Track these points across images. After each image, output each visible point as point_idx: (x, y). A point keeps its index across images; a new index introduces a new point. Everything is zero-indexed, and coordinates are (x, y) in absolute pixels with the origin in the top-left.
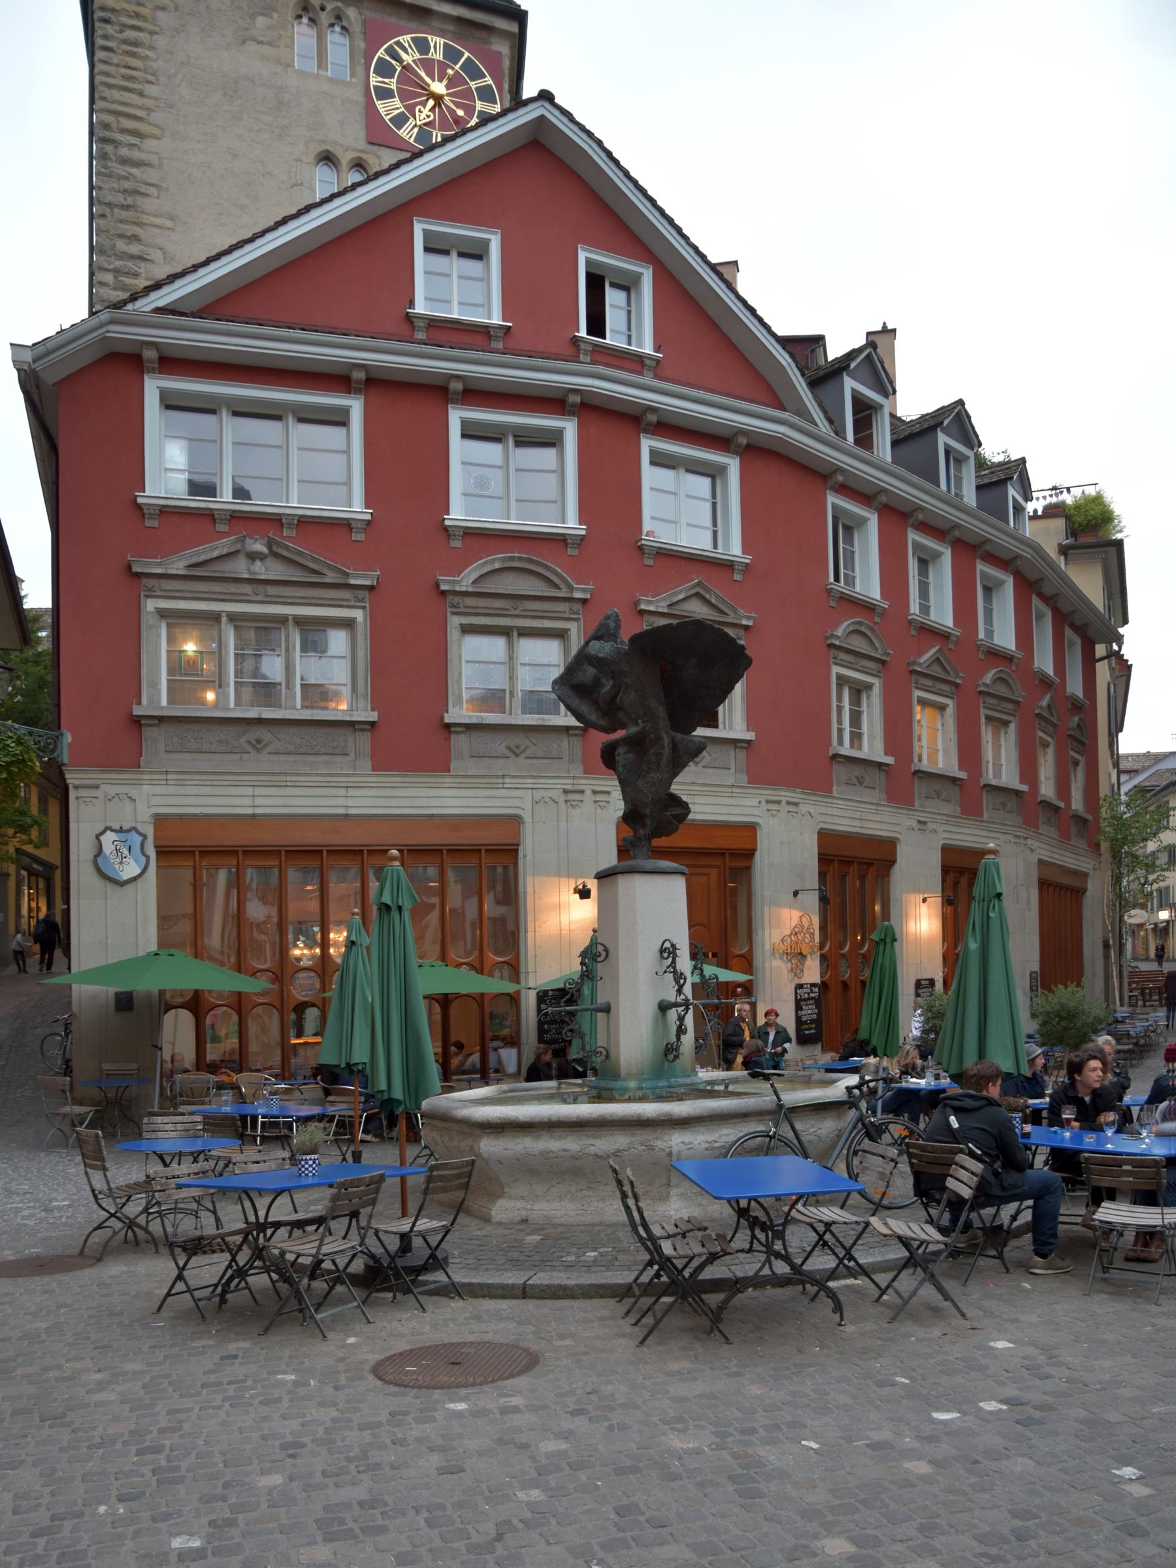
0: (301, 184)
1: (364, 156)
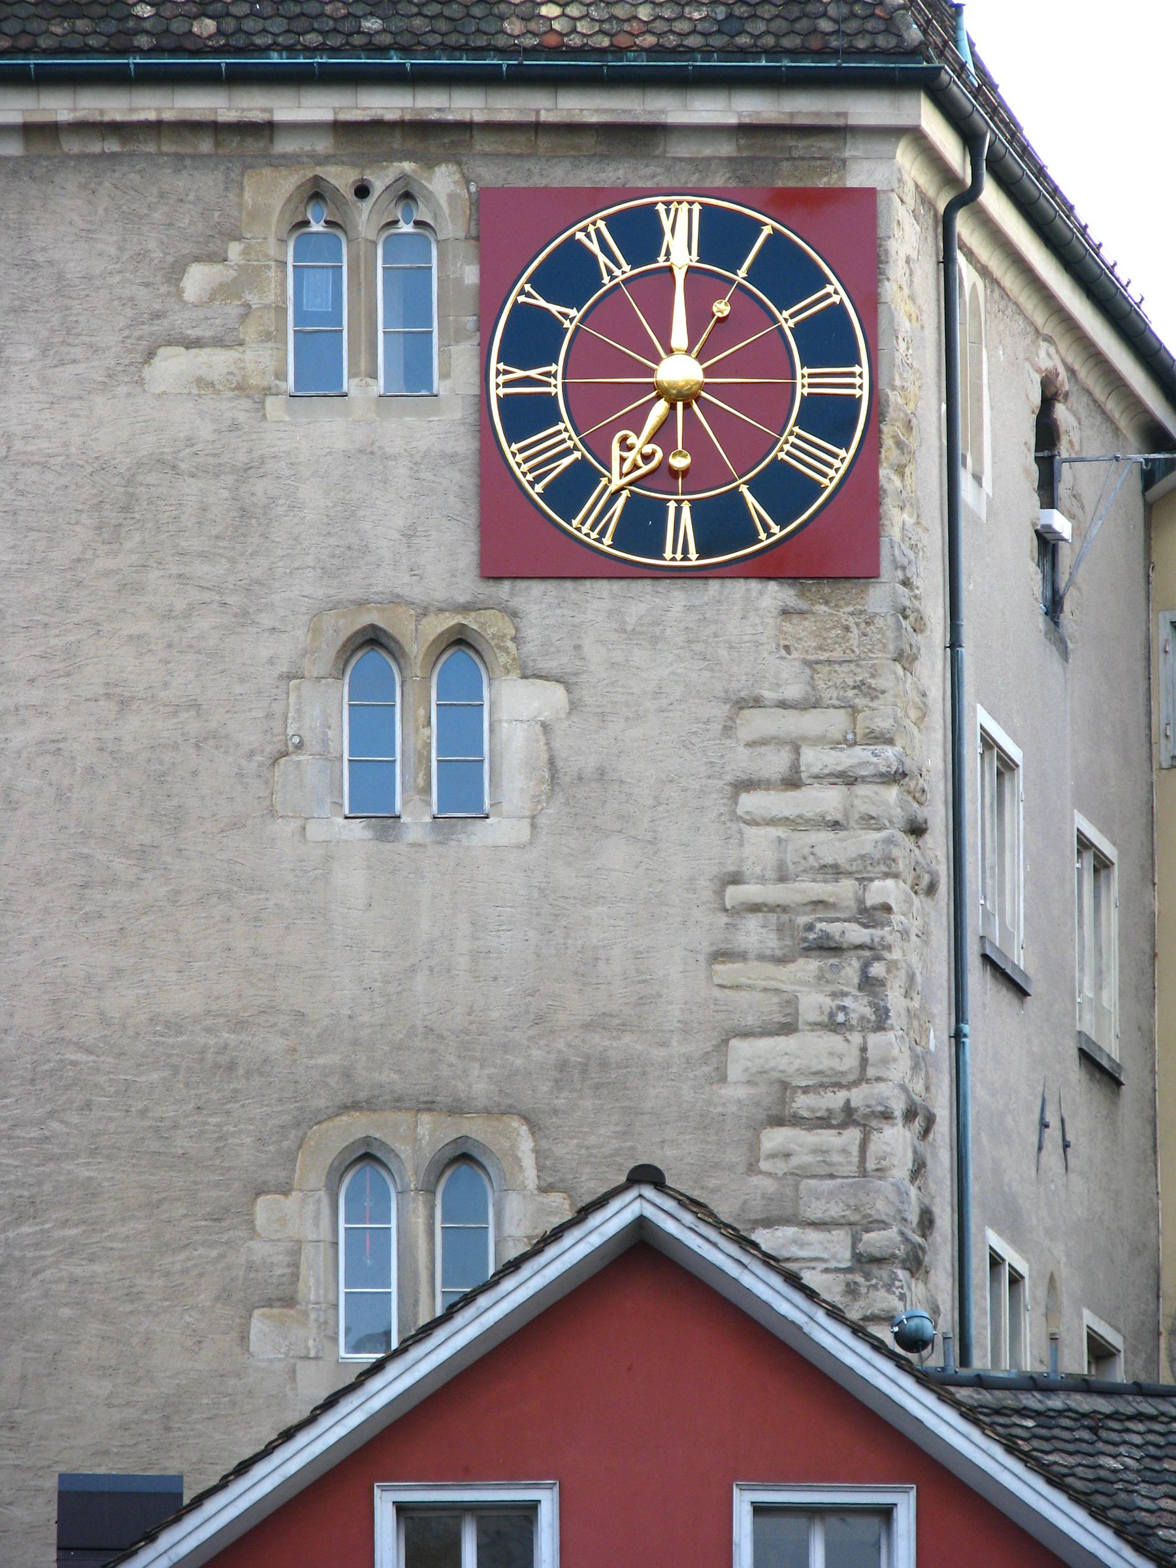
0: (299, 746)
1: (471, 621)
